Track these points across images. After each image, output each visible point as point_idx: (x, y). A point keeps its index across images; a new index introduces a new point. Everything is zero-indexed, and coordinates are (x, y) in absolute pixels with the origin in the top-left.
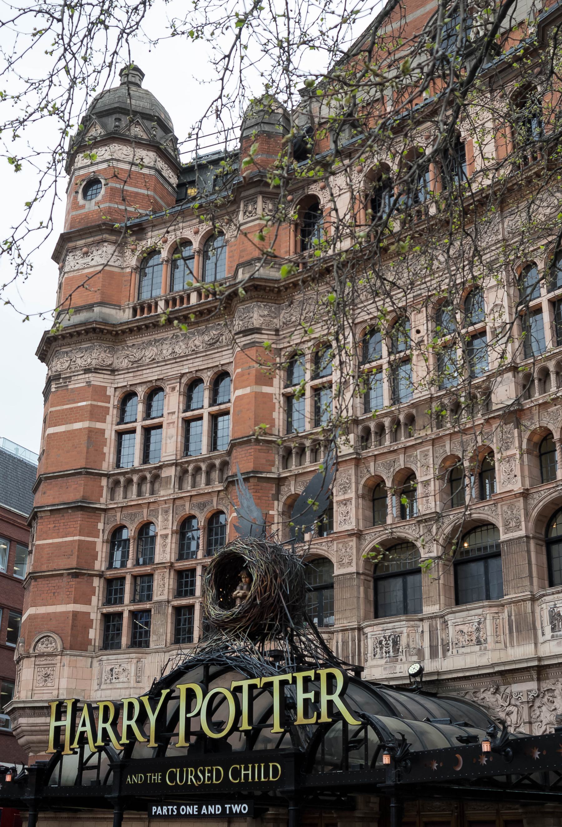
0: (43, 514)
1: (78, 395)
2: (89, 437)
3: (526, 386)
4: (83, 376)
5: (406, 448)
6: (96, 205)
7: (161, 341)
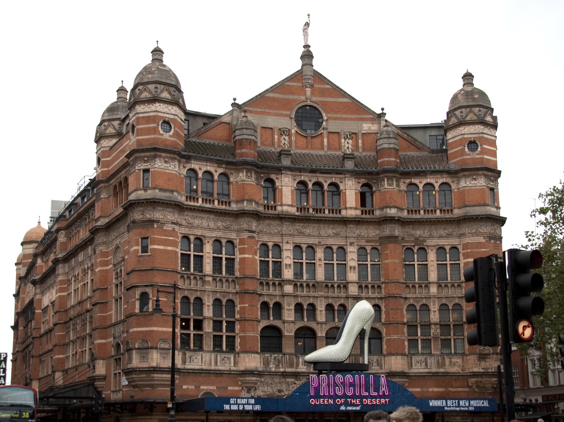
1: (167, 233)
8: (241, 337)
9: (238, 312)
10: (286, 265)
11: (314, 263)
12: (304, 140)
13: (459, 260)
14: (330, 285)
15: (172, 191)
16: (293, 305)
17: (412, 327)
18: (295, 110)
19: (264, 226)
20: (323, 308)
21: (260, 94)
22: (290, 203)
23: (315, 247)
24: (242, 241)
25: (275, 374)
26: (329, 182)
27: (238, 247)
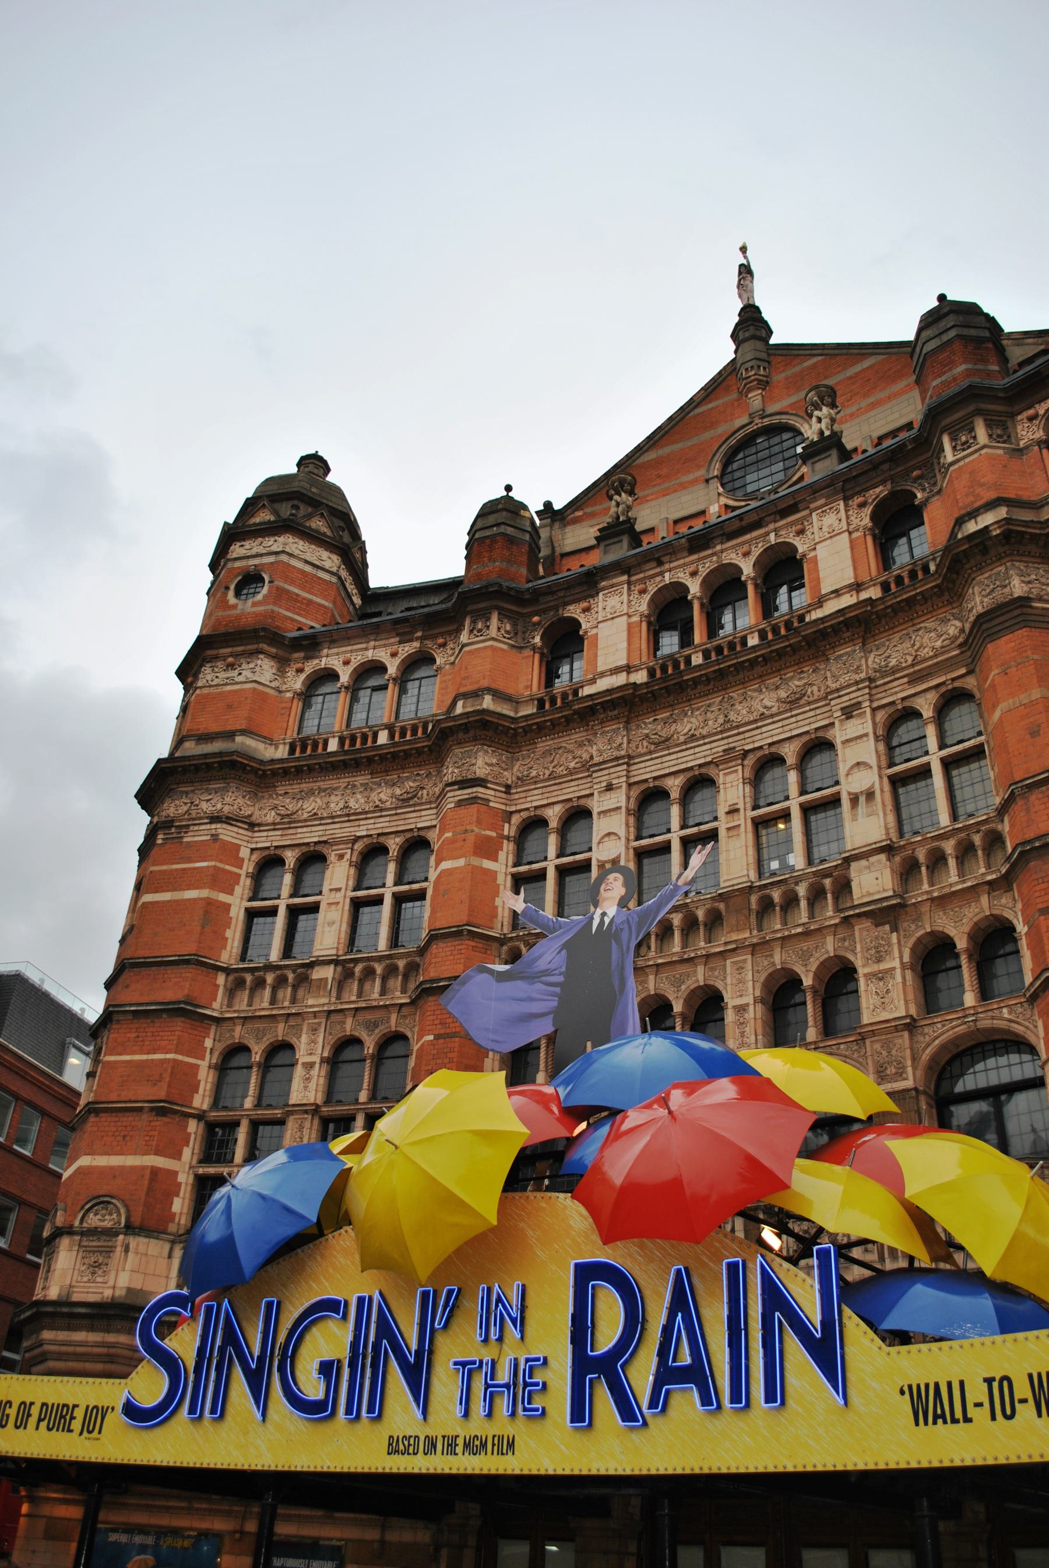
0: (121, 1017)
2: (206, 912)
3: (908, 871)
4: (208, 827)
5: (708, 956)
6: (251, 607)
7: (330, 791)
15: (230, 735)
19: (532, 763)
22: (623, 662)
23: (712, 772)
26: (756, 552)
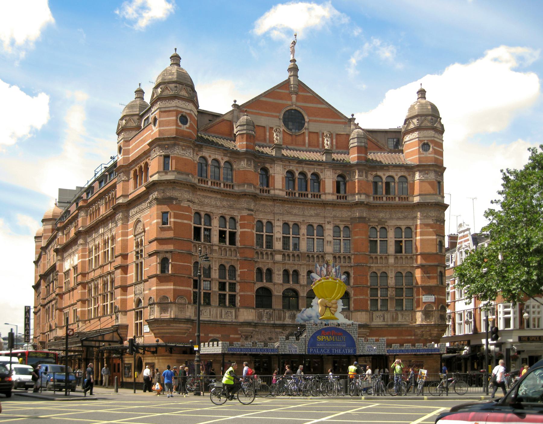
8: (240, 296)
9: (239, 276)
10: (277, 238)
11: (299, 238)
12: (290, 138)
13: (412, 238)
14: (311, 255)
15: (188, 175)
16: (282, 271)
17: (374, 290)
18: (283, 112)
20: (305, 274)
21: (255, 98)
22: (281, 188)
23: (299, 224)
24: (243, 218)
25: (267, 325)
26: (312, 172)
27: (239, 222)
